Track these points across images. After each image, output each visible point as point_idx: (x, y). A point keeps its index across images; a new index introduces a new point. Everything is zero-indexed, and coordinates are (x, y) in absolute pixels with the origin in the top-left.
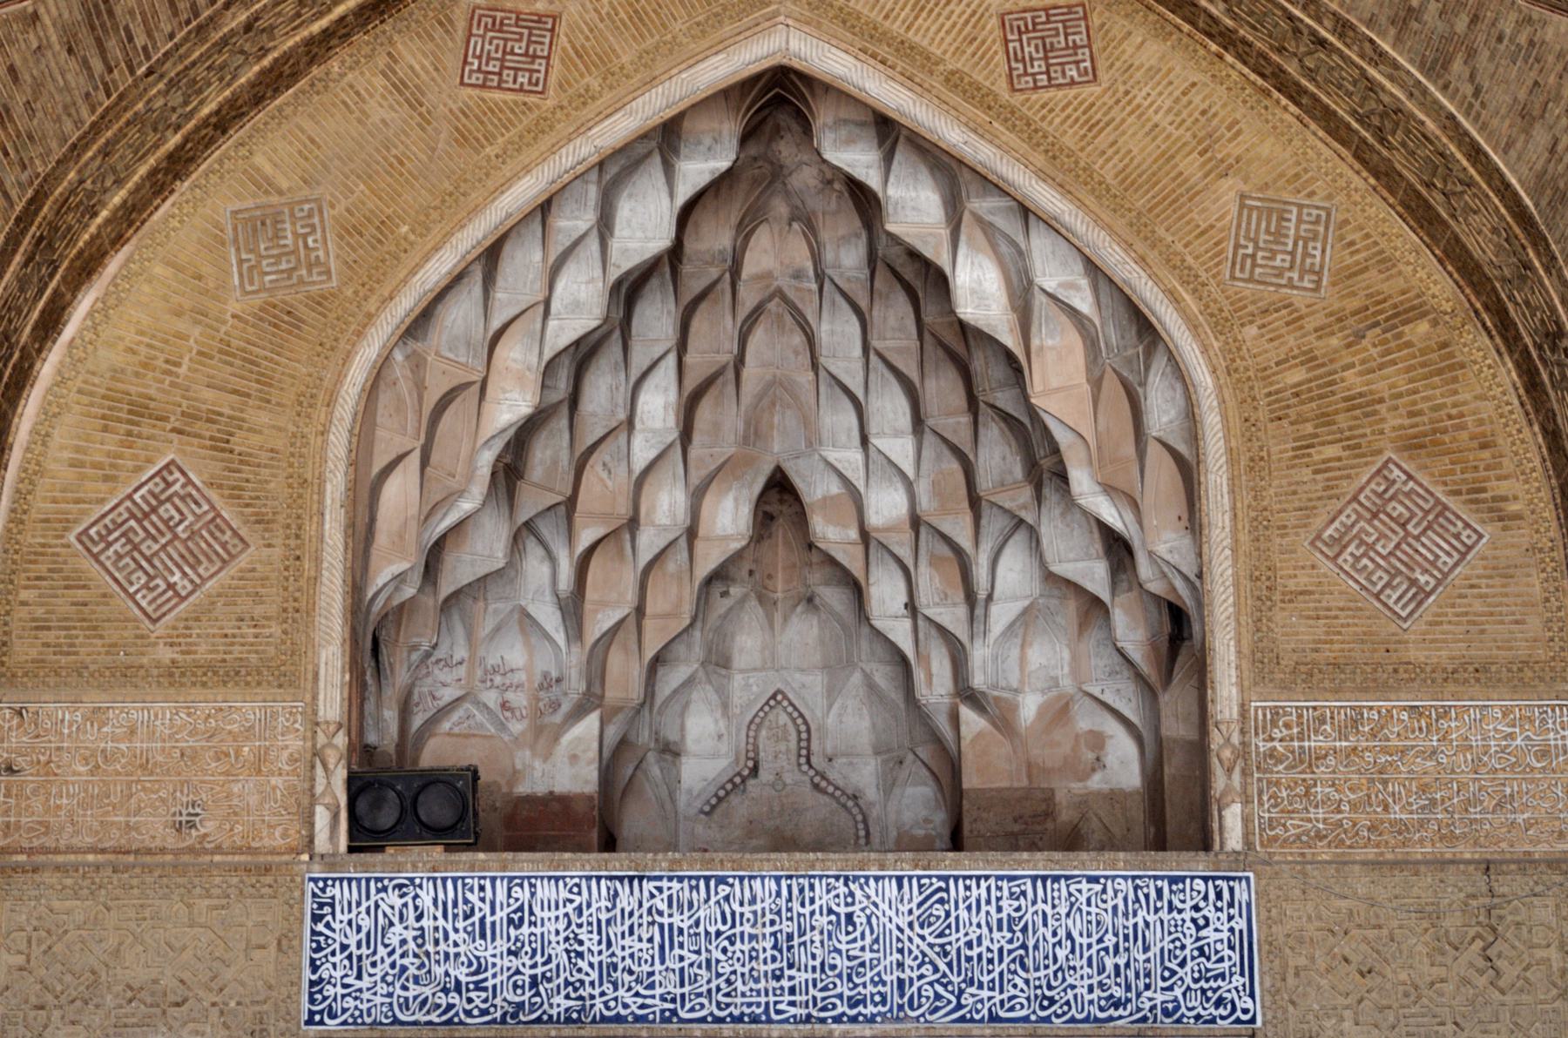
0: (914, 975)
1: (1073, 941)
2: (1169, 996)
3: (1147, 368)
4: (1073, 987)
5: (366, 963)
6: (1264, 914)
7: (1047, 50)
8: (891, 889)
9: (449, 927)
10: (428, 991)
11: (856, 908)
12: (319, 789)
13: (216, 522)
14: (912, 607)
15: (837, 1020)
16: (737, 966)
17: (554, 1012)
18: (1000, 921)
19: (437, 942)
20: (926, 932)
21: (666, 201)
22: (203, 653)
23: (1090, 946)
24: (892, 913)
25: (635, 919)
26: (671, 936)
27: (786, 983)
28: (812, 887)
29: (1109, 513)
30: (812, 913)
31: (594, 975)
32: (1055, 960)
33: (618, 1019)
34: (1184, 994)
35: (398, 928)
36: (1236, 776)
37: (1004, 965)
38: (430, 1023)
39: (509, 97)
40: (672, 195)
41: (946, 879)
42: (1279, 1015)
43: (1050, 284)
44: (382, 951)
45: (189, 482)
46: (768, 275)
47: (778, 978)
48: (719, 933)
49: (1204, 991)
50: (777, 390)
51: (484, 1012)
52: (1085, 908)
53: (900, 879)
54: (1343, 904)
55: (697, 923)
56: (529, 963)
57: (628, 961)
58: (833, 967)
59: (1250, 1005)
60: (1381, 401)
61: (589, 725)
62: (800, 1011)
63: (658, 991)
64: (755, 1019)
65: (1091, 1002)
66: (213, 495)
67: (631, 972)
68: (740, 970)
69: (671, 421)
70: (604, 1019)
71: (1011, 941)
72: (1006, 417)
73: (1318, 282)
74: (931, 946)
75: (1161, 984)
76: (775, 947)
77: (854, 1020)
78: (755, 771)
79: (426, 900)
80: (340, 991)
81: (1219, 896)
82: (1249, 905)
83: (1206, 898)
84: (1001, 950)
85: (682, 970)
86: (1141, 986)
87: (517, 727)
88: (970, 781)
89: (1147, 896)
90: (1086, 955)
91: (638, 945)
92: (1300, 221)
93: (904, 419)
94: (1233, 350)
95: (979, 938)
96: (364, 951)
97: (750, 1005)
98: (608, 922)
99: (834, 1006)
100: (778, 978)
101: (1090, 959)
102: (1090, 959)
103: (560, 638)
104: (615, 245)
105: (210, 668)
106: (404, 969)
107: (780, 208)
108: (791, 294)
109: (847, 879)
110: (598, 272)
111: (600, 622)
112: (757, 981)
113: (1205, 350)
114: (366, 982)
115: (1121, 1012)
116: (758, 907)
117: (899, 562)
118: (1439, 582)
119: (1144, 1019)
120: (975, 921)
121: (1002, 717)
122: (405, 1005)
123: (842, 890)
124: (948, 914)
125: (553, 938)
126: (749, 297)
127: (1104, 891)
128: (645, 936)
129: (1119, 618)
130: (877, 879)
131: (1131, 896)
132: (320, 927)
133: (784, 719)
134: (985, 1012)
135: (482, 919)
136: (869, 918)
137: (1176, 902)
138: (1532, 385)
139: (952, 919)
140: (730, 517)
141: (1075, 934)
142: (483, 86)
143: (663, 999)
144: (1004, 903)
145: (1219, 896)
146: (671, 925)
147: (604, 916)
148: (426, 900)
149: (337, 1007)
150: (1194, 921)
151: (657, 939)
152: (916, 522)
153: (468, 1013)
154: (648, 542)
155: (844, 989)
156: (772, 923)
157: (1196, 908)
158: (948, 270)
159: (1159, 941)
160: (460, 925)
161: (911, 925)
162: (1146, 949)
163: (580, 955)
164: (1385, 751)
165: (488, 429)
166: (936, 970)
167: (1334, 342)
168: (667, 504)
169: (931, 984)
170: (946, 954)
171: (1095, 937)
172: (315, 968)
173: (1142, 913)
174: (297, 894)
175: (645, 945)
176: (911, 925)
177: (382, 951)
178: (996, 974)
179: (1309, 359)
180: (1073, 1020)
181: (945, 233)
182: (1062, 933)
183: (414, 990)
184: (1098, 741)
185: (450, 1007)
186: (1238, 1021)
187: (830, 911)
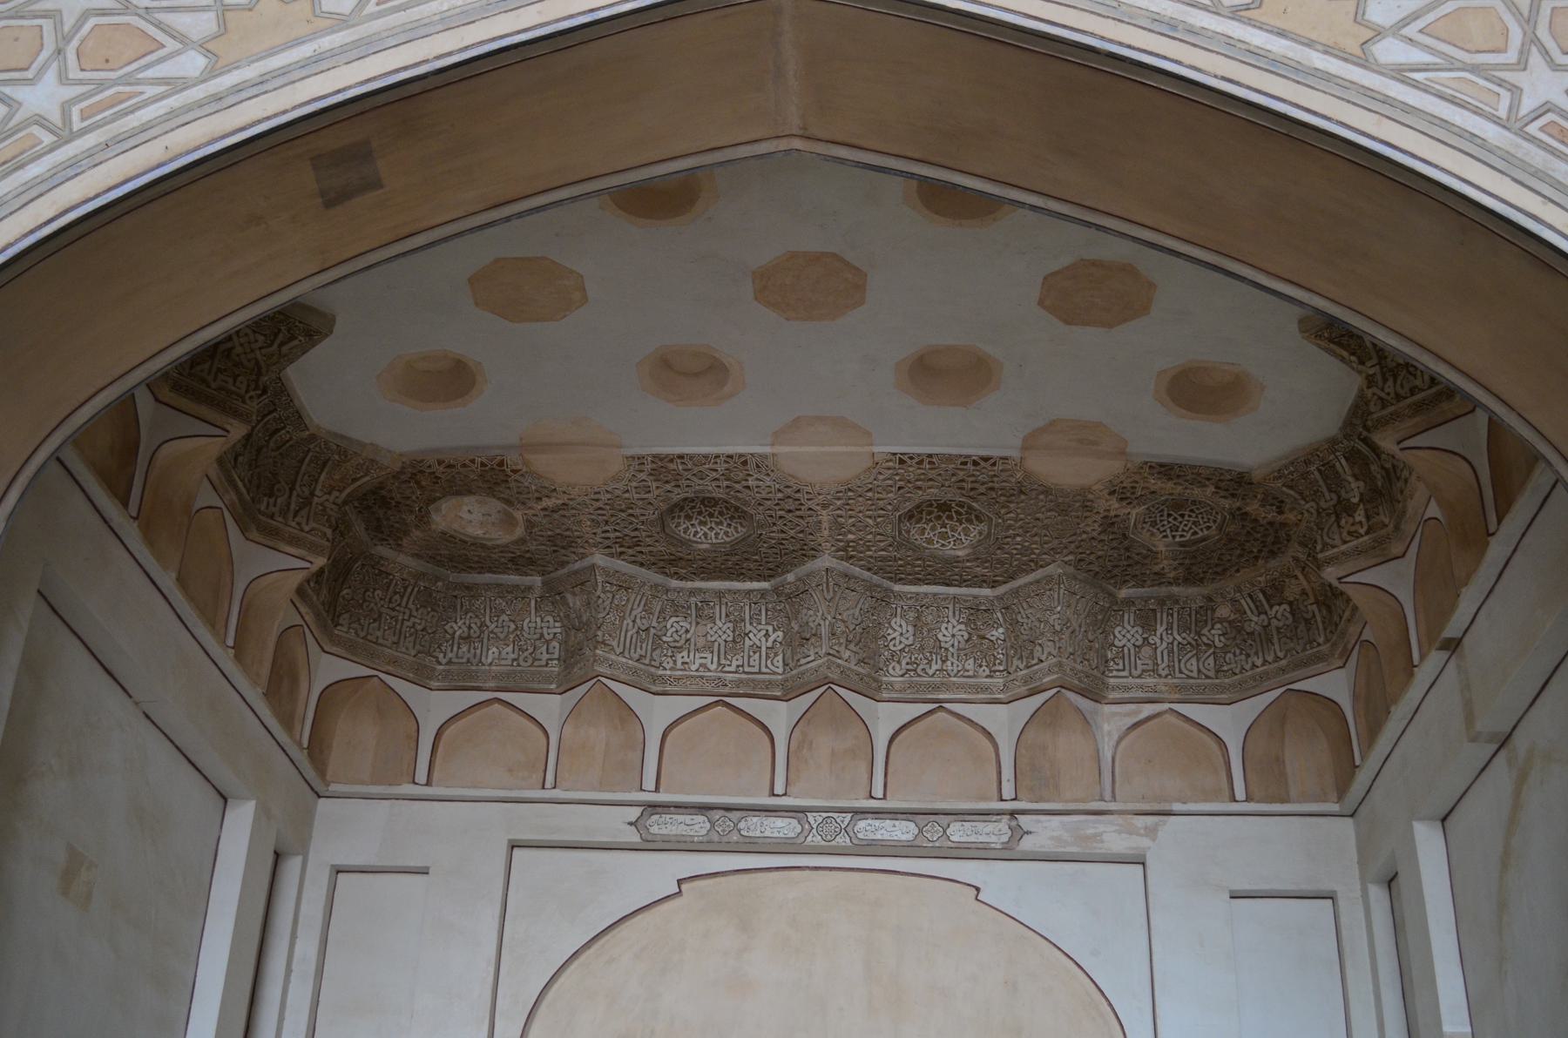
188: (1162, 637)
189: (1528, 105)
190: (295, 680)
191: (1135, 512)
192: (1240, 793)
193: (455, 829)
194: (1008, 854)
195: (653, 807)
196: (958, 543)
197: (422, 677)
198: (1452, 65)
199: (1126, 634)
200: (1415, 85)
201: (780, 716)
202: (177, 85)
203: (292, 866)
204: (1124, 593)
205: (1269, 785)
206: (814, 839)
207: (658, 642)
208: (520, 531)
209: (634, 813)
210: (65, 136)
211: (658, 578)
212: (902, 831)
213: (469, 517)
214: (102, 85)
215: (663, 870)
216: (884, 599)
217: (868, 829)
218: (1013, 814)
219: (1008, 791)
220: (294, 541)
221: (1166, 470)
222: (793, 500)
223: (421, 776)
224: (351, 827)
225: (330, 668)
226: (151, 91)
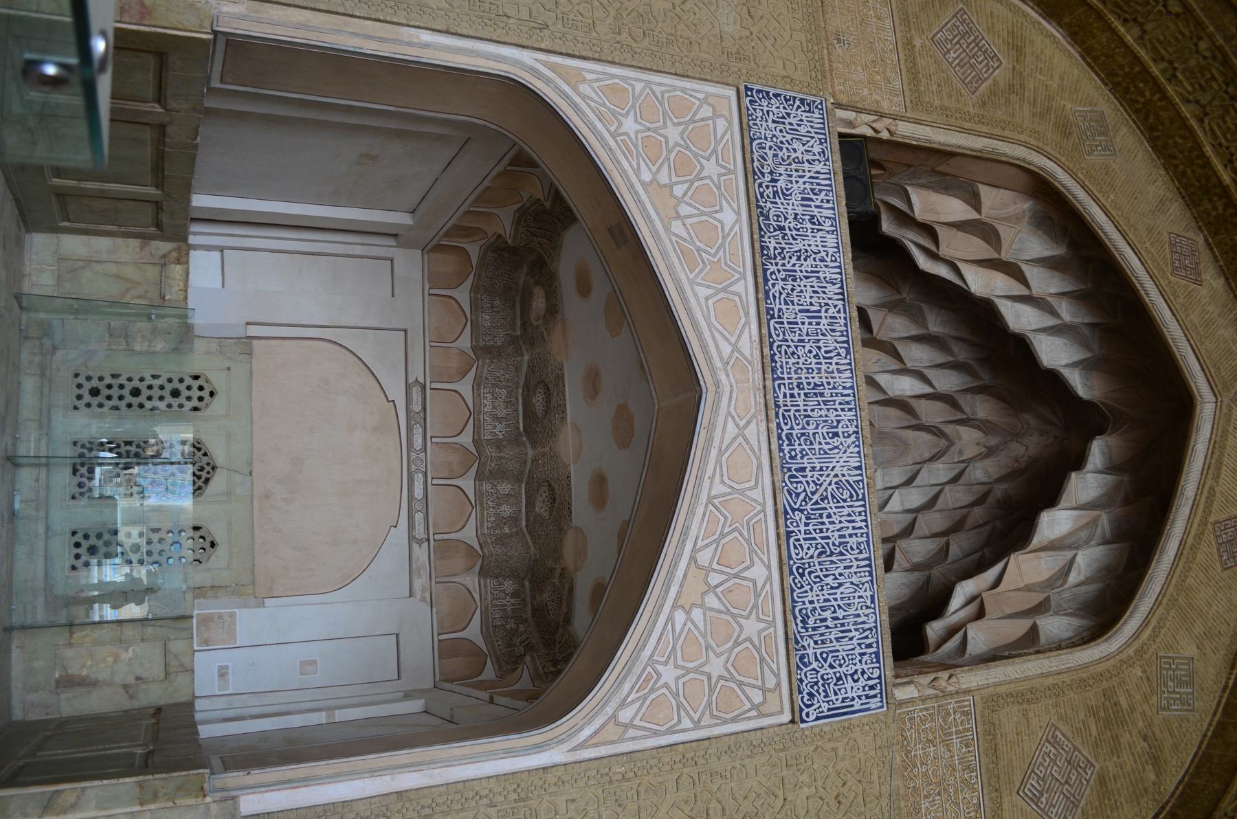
0: (809, 479)
1: (837, 588)
2: (812, 658)
4: (811, 590)
5: (781, 127)
6: (865, 721)
9: (806, 179)
10: (770, 162)
11: (842, 439)
13: (980, 79)
16: (802, 360)
17: (766, 239)
18: (844, 536)
19: (797, 171)
20: (833, 486)
21: (1064, 362)
22: (921, 62)
23: (836, 600)
24: (841, 463)
25: (822, 295)
26: (815, 316)
27: (796, 391)
28: (850, 410)
30: (836, 410)
31: (789, 267)
32: (826, 576)
33: (766, 280)
34: (814, 669)
35: (802, 149)
37: (820, 540)
38: (753, 161)
41: (863, 499)
42: (809, 740)
43: (1079, 559)
44: (789, 137)
45: (995, 70)
46: (960, 438)
47: (798, 386)
48: (819, 348)
49: (816, 683)
50: (904, 446)
51: (762, 195)
52: (857, 594)
53: (859, 468)
54: (875, 777)
55: (823, 335)
56: (792, 226)
57: (798, 289)
58: (808, 424)
59: (812, 717)
60: (1118, 757)
63: (784, 307)
64: (774, 370)
65: (804, 603)
66: (990, 81)
67: (793, 290)
68: (801, 361)
70: (765, 271)
71: (834, 544)
72: (946, 549)
73: (1163, 709)
74: (826, 490)
75: (819, 651)
76: (815, 385)
77: (780, 438)
80: (765, 109)
81: (872, 688)
82: (868, 709)
83: (869, 678)
84: (828, 538)
85: (797, 323)
86: (816, 638)
89: (867, 637)
90: (830, 597)
91: (808, 295)
94: (1129, 663)
95: (833, 523)
97: (782, 367)
98: (818, 278)
99: (786, 424)
100: (798, 386)
101: (828, 600)
102: (828, 600)
105: (915, 65)
106: (781, 149)
107: (993, 441)
108: (952, 449)
109: (856, 433)
110: (1034, 327)
112: (796, 372)
115: (800, 625)
116: (836, 375)
119: (797, 642)
120: (843, 519)
123: (851, 430)
124: (845, 501)
125: (806, 242)
126: (949, 429)
127: (867, 607)
128: (813, 300)
130: (859, 452)
131: (866, 626)
132: (798, 103)
134: (792, 529)
135: (811, 200)
136: (837, 447)
137: (866, 658)
139: (842, 504)
141: (842, 589)
143: (780, 310)
144: (854, 539)
145: (872, 688)
146: (820, 317)
147: (821, 275)
148: (819, 167)
150: (856, 671)
151: (812, 308)
153: (760, 185)
156: (829, 383)
157: (863, 672)
159: (843, 647)
161: (836, 476)
162: (837, 639)
163: (799, 259)
164: (956, 791)
165: (966, 269)
166: (813, 493)
167: (1141, 723)
169: (805, 490)
170: (822, 500)
171: (841, 603)
172: (776, 95)
174: (814, 92)
175: (808, 300)
176: (836, 476)
177: (789, 137)
178: (814, 535)
179: (1132, 709)
180: (793, 591)
182: (842, 580)
185: (763, 174)
186: (801, 710)
187: (838, 422)
188: (508, 601)
189: (660, 668)
190: (466, 236)
191: (556, 580)
192: (441, 637)
193: (412, 307)
194: (411, 538)
195: (424, 388)
196: (541, 508)
197: (475, 289)
198: (676, 640)
199: (509, 586)
200: (666, 625)
201: (466, 439)
202: (637, 172)
203: (392, 242)
204: (527, 583)
205: (447, 650)
206: (413, 456)
207: (494, 386)
208: (535, 323)
209: (421, 380)
211: (522, 384)
212: (418, 492)
213: (539, 303)
214: (636, 146)
215: (397, 392)
216: (518, 480)
217: (419, 478)
218: (428, 540)
219: (438, 537)
220: (516, 231)
221: (571, 590)
222: (552, 435)
223: (432, 291)
224: (410, 264)
225: (474, 250)
226: (634, 164)
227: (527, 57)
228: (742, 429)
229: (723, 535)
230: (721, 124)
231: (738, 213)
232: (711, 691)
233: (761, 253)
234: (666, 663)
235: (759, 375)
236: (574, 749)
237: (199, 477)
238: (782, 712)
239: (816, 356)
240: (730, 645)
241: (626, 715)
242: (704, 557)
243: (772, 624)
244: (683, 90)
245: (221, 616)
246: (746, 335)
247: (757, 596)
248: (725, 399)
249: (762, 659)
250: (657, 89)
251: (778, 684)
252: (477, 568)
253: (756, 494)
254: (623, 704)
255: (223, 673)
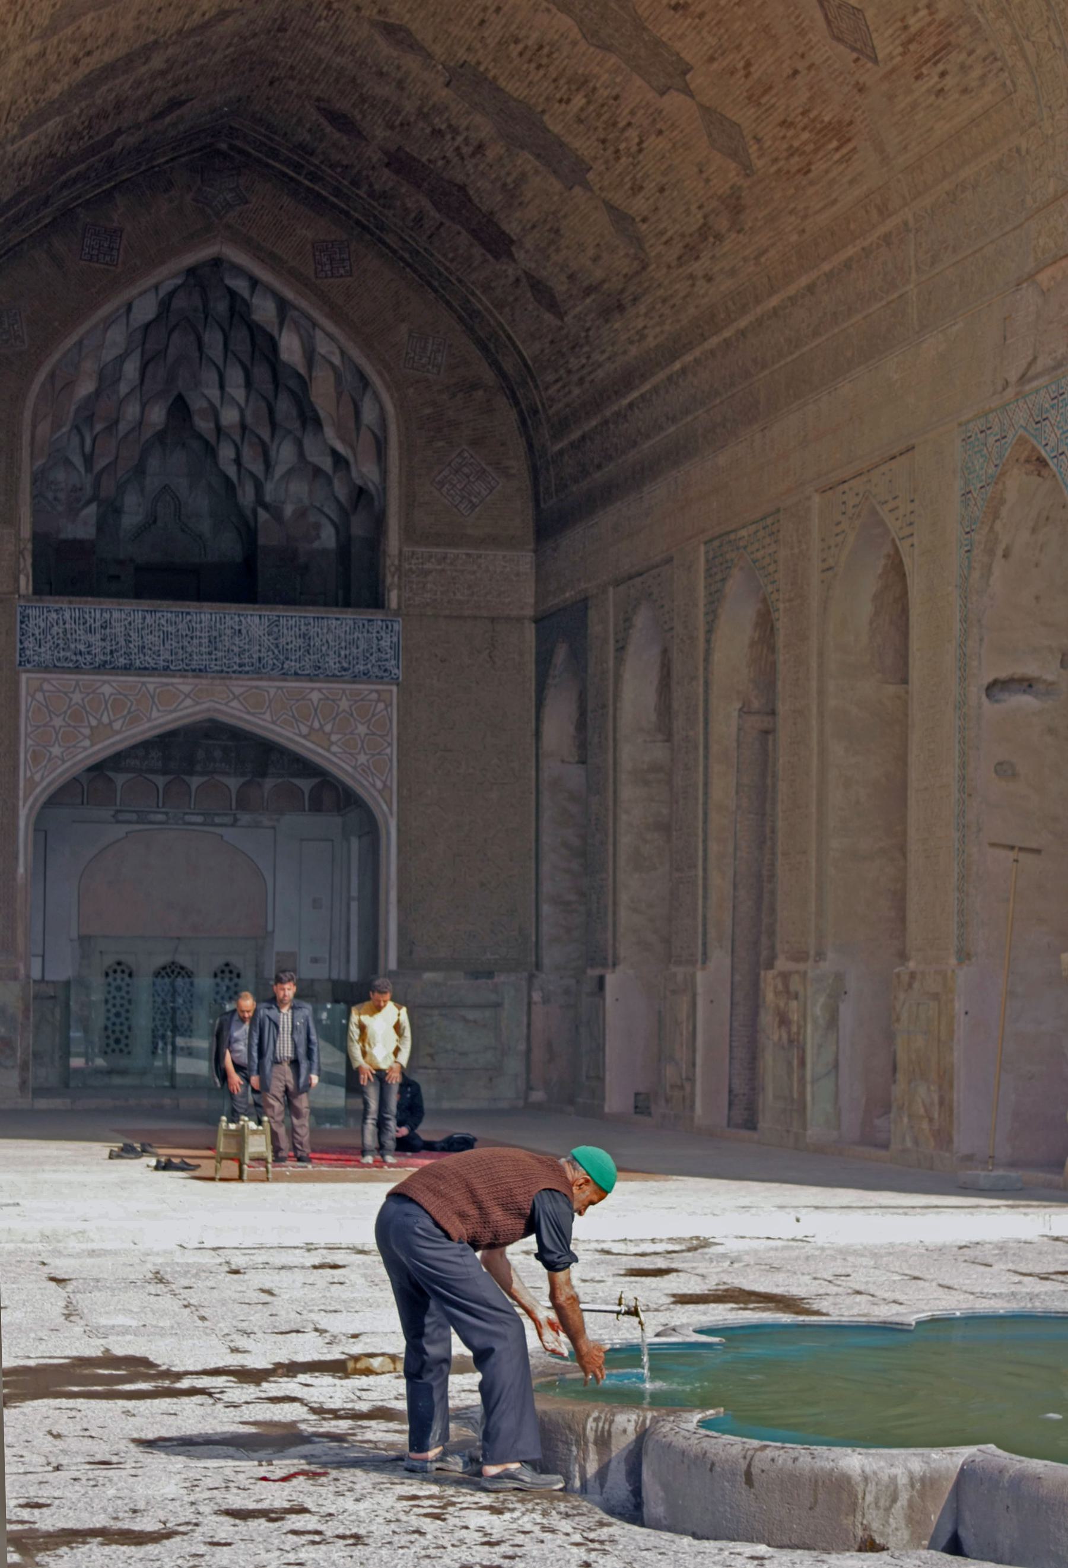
3: (364, 394)
5: (43, 642)
7: (331, 260)
8: (257, 620)
12: (22, 566)
14: (238, 461)
15: (234, 672)
26: (167, 635)
27: (213, 657)
29: (340, 447)
31: (136, 650)
33: (146, 669)
36: (396, 579)
39: (102, 266)
40: (157, 294)
41: (279, 616)
51: (91, 664)
53: (260, 616)
61: (93, 508)
62: (218, 668)
63: (162, 658)
69: (137, 375)
72: (292, 392)
77: (240, 672)
78: (155, 522)
79: (67, 616)
81: (387, 627)
87: (60, 508)
88: (261, 541)
92: (433, 344)
93: (241, 380)
96: (42, 637)
103: (82, 470)
104: (132, 316)
106: (58, 645)
111: (100, 464)
113: (392, 397)
114: (43, 650)
117: (234, 442)
118: (481, 502)
121: (276, 513)
122: (59, 659)
129: (336, 483)
132: (24, 626)
133: (168, 498)
138: (523, 422)
140: (157, 415)
142: (90, 260)
144: (302, 627)
145: (387, 627)
147: (140, 626)
148: (67, 616)
149: (31, 659)
152: (243, 427)
154: (123, 428)
155: (237, 659)
158: (277, 337)
160: (81, 627)
164: (456, 571)
168: (132, 411)
172: (21, 642)
173: (356, 634)
177: (49, 637)
181: (276, 320)
183: (62, 654)
184: (317, 526)
185: (77, 661)
194: (233, 825)
198: (345, 752)
201: (161, 781)
202: (85, 749)
209: (112, 813)
210: (64, 762)
212: (199, 819)
215: (121, 830)
227: (23, 813)
228: (235, 697)
229: (293, 717)
230: (46, 686)
231: (104, 682)
232: (374, 734)
233: (127, 669)
234: (357, 760)
235: (204, 681)
236: (391, 814)
237: (179, 973)
238: (391, 691)
239: (192, 638)
240: (352, 720)
241: (379, 785)
242: (305, 730)
243: (344, 690)
244: (27, 711)
245: (278, 962)
246: (181, 687)
247: (328, 699)
248: (218, 706)
249: (362, 700)
250: (29, 729)
251: (377, 691)
252: (259, 780)
253: (272, 691)
254: (374, 786)
255: (315, 960)
